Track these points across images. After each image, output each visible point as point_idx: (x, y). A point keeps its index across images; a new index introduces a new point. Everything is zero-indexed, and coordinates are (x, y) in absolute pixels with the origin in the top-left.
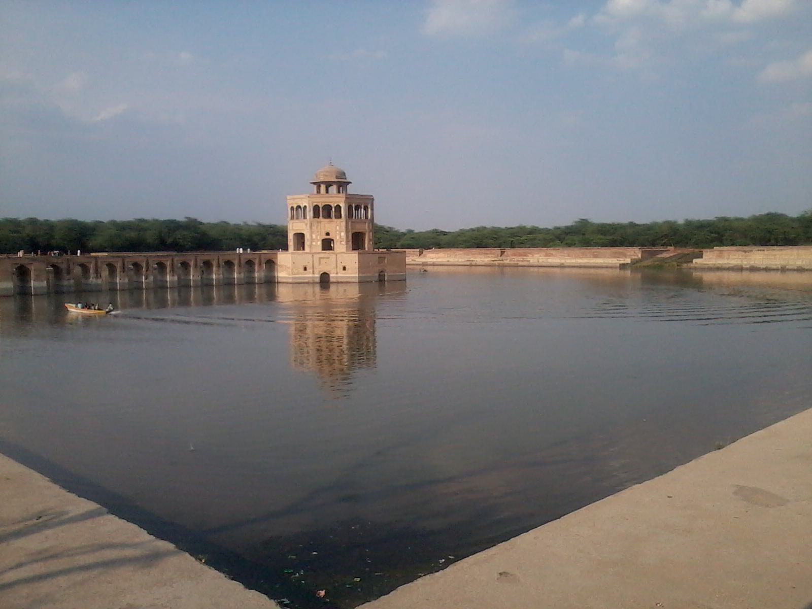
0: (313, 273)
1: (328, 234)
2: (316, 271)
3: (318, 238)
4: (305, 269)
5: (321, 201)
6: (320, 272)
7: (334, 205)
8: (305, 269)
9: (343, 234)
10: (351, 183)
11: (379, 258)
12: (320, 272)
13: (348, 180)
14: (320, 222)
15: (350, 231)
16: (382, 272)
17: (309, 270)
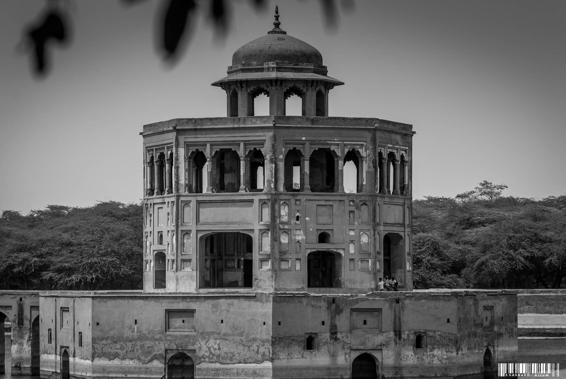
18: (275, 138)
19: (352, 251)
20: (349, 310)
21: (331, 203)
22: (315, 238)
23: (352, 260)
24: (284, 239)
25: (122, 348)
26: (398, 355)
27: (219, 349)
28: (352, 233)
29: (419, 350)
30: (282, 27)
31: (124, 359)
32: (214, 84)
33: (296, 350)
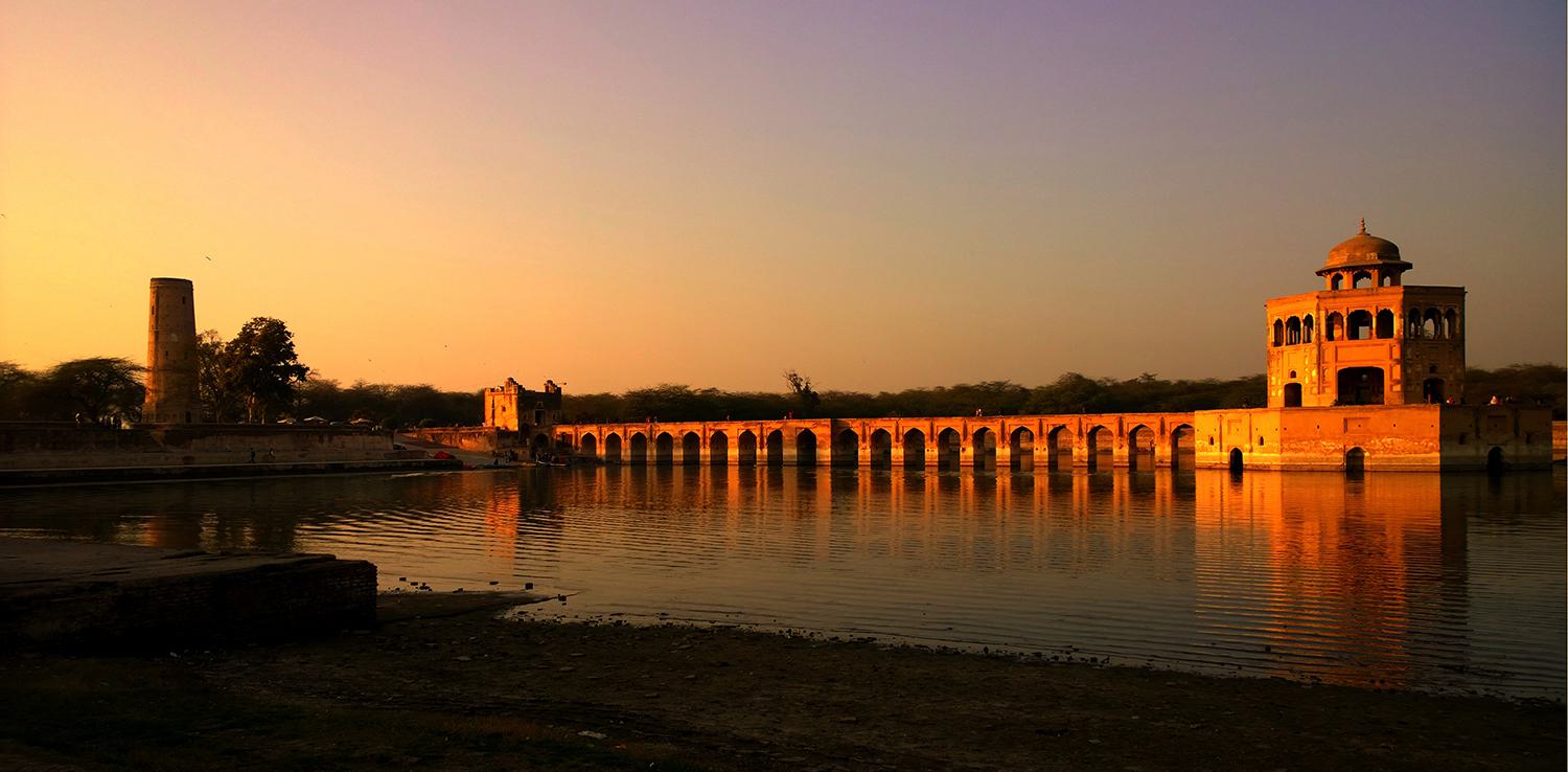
1: (1293, 375)
2: (1224, 448)
3: (1279, 383)
4: (1212, 442)
5: (1345, 307)
8: (1212, 442)
9: (1314, 373)
10: (1409, 266)
11: (1346, 420)
13: (1404, 258)
17: (1217, 444)
18: (1404, 300)
19: (1451, 379)
22: (1428, 370)
24: (1409, 371)
28: (1451, 366)
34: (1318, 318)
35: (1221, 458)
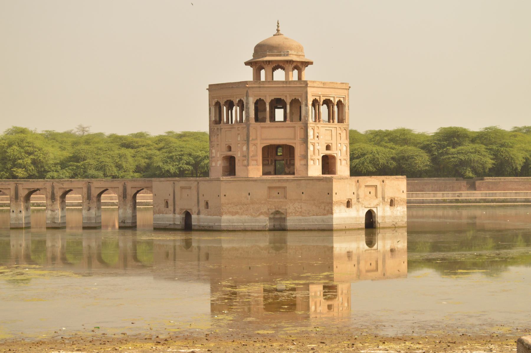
0: (174, 212)
1: (230, 149)
2: (177, 210)
6: (181, 209)
7: (236, 101)
9: (245, 148)
10: (311, 63)
12: (181, 209)
14: (221, 129)
15: (258, 142)
16: (277, 212)
20: (364, 186)
21: (331, 129)
23: (340, 160)
25: (241, 209)
26: (384, 210)
27: (301, 208)
29: (392, 207)
30: (281, 32)
31: (242, 214)
32: (247, 64)
33: (344, 207)
34: (247, 103)
35: (174, 219)
